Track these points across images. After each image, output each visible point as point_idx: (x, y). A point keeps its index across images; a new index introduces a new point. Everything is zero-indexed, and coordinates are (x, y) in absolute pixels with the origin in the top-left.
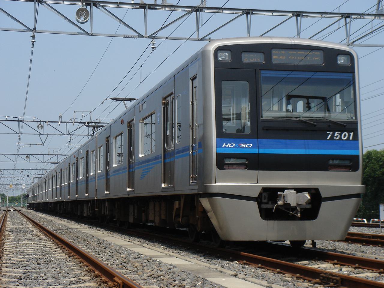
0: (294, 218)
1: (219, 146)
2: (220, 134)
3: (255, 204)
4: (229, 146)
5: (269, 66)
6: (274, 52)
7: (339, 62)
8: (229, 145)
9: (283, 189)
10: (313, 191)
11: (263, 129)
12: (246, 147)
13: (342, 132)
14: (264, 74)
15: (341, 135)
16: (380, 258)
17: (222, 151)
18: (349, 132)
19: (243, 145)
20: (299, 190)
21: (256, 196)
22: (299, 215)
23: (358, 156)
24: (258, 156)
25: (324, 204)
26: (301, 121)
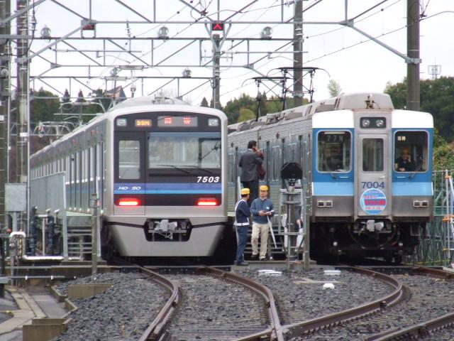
0: (168, 240)
1: (116, 188)
2: (117, 180)
3: (142, 231)
4: (123, 189)
5: (155, 128)
6: (160, 118)
7: (210, 124)
8: (123, 188)
9: (160, 220)
10: (187, 221)
11: (148, 175)
12: (136, 189)
13: (209, 176)
14: (152, 134)
15: (208, 179)
16: (141, 271)
17: (118, 192)
18: (215, 176)
19: (134, 188)
20: (171, 220)
21: (143, 224)
22: (172, 238)
23: (221, 194)
24: (145, 196)
25: (193, 230)
26: (178, 169)
